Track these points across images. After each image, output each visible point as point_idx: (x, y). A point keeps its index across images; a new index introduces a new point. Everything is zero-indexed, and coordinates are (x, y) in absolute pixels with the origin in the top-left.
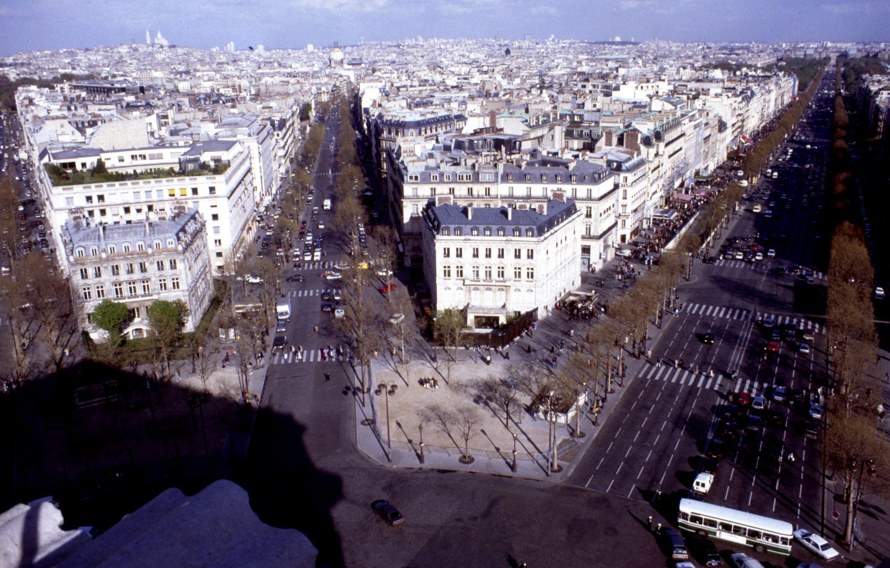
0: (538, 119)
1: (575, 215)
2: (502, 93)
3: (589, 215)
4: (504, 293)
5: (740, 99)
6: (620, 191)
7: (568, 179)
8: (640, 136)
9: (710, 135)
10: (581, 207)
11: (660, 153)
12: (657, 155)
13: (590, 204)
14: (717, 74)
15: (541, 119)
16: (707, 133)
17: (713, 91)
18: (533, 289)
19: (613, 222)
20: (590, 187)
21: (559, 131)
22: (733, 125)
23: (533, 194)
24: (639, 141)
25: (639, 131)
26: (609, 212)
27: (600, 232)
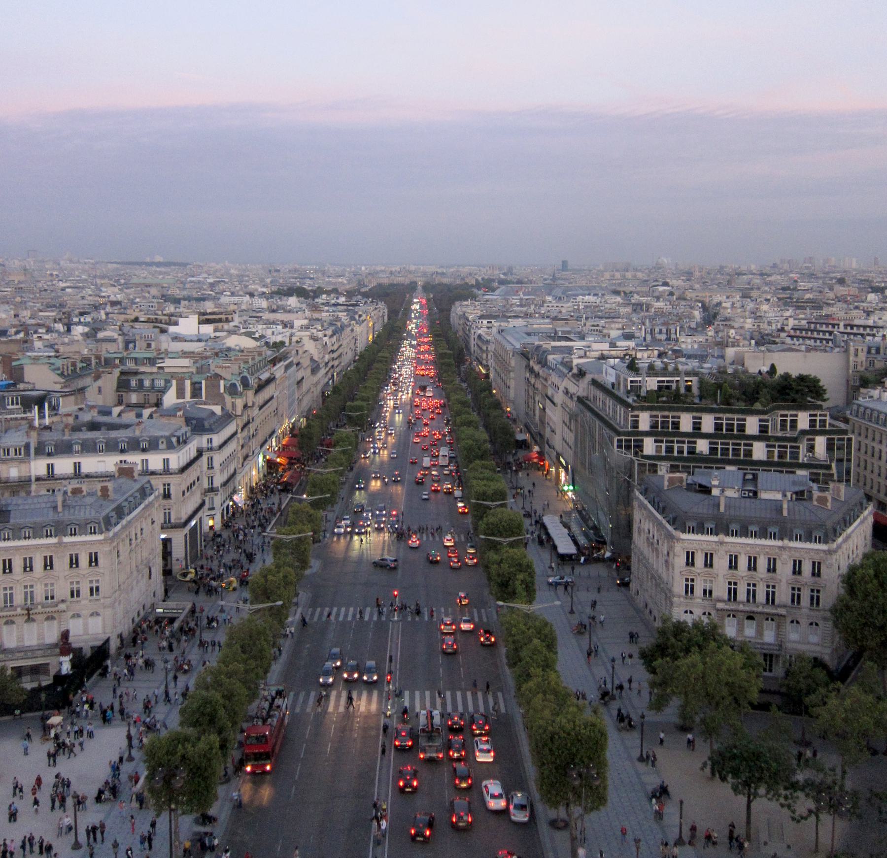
0: (74, 364)
1: (152, 498)
2: (13, 330)
3: (167, 496)
4: (55, 622)
5: (329, 332)
6: (204, 459)
7: (134, 445)
8: (222, 382)
9: (303, 378)
10: (158, 483)
11: (250, 404)
12: (245, 406)
13: (167, 479)
14: (293, 301)
15: (79, 365)
16: (299, 376)
17: (298, 323)
18: (101, 611)
19: (199, 501)
20: (166, 456)
21: (109, 381)
22: (326, 364)
23: (85, 470)
24: (222, 390)
25: (221, 377)
26: (194, 488)
27: (184, 517)
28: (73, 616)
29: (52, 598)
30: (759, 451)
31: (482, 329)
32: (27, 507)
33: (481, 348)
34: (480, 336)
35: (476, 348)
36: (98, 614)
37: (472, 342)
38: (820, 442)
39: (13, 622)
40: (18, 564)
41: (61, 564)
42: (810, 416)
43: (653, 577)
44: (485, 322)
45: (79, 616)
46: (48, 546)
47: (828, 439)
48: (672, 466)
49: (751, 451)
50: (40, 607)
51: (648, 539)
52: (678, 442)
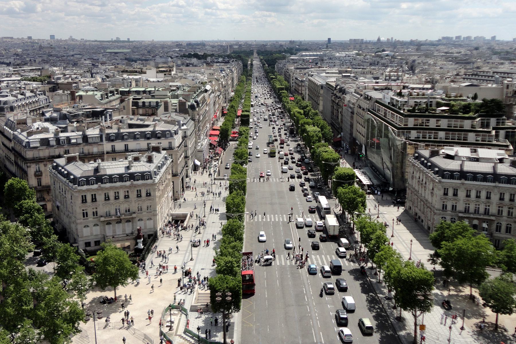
4: (131, 223)
18: (152, 217)
28: (139, 220)
29: (129, 211)
30: (471, 137)
31: (298, 75)
32: (113, 167)
33: (298, 85)
34: (296, 79)
35: (294, 84)
36: (151, 219)
37: (292, 81)
38: (502, 133)
39: (111, 224)
40: (112, 195)
41: (133, 195)
42: (497, 120)
43: (421, 200)
44: (298, 70)
45: (142, 220)
46: (126, 187)
47: (507, 132)
48: (427, 145)
49: (467, 137)
50: (123, 216)
51: (419, 181)
52: (429, 133)
